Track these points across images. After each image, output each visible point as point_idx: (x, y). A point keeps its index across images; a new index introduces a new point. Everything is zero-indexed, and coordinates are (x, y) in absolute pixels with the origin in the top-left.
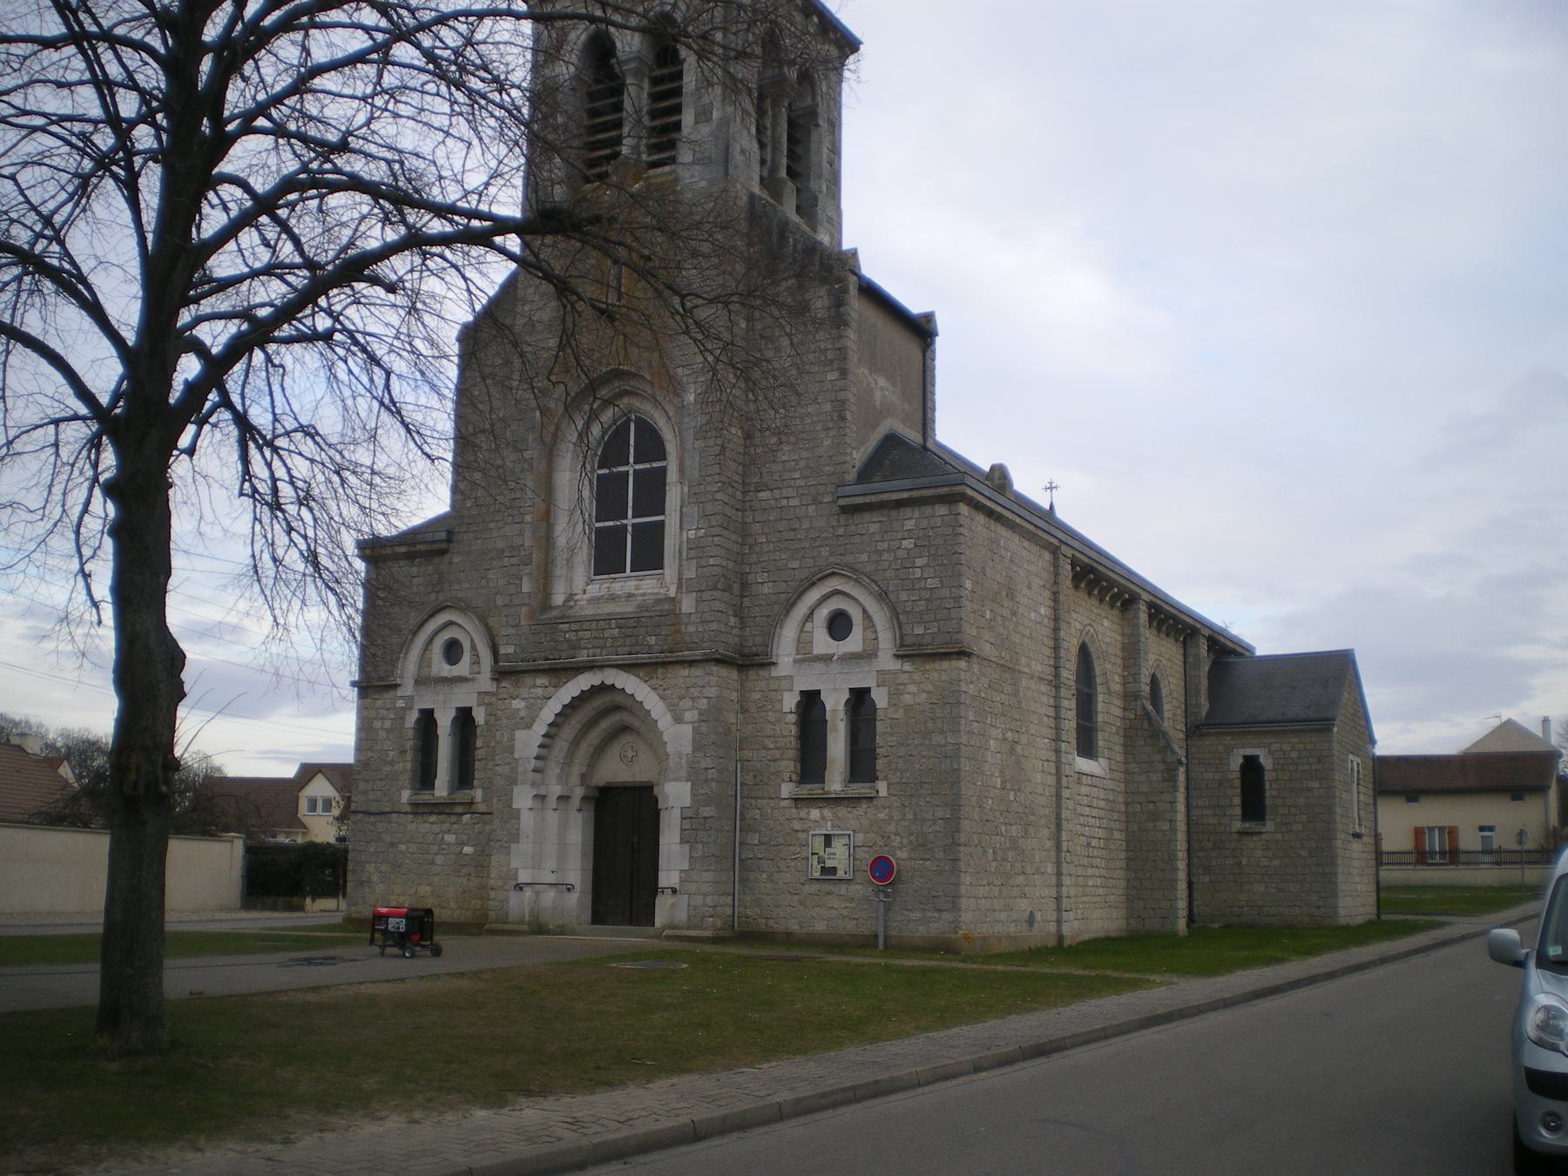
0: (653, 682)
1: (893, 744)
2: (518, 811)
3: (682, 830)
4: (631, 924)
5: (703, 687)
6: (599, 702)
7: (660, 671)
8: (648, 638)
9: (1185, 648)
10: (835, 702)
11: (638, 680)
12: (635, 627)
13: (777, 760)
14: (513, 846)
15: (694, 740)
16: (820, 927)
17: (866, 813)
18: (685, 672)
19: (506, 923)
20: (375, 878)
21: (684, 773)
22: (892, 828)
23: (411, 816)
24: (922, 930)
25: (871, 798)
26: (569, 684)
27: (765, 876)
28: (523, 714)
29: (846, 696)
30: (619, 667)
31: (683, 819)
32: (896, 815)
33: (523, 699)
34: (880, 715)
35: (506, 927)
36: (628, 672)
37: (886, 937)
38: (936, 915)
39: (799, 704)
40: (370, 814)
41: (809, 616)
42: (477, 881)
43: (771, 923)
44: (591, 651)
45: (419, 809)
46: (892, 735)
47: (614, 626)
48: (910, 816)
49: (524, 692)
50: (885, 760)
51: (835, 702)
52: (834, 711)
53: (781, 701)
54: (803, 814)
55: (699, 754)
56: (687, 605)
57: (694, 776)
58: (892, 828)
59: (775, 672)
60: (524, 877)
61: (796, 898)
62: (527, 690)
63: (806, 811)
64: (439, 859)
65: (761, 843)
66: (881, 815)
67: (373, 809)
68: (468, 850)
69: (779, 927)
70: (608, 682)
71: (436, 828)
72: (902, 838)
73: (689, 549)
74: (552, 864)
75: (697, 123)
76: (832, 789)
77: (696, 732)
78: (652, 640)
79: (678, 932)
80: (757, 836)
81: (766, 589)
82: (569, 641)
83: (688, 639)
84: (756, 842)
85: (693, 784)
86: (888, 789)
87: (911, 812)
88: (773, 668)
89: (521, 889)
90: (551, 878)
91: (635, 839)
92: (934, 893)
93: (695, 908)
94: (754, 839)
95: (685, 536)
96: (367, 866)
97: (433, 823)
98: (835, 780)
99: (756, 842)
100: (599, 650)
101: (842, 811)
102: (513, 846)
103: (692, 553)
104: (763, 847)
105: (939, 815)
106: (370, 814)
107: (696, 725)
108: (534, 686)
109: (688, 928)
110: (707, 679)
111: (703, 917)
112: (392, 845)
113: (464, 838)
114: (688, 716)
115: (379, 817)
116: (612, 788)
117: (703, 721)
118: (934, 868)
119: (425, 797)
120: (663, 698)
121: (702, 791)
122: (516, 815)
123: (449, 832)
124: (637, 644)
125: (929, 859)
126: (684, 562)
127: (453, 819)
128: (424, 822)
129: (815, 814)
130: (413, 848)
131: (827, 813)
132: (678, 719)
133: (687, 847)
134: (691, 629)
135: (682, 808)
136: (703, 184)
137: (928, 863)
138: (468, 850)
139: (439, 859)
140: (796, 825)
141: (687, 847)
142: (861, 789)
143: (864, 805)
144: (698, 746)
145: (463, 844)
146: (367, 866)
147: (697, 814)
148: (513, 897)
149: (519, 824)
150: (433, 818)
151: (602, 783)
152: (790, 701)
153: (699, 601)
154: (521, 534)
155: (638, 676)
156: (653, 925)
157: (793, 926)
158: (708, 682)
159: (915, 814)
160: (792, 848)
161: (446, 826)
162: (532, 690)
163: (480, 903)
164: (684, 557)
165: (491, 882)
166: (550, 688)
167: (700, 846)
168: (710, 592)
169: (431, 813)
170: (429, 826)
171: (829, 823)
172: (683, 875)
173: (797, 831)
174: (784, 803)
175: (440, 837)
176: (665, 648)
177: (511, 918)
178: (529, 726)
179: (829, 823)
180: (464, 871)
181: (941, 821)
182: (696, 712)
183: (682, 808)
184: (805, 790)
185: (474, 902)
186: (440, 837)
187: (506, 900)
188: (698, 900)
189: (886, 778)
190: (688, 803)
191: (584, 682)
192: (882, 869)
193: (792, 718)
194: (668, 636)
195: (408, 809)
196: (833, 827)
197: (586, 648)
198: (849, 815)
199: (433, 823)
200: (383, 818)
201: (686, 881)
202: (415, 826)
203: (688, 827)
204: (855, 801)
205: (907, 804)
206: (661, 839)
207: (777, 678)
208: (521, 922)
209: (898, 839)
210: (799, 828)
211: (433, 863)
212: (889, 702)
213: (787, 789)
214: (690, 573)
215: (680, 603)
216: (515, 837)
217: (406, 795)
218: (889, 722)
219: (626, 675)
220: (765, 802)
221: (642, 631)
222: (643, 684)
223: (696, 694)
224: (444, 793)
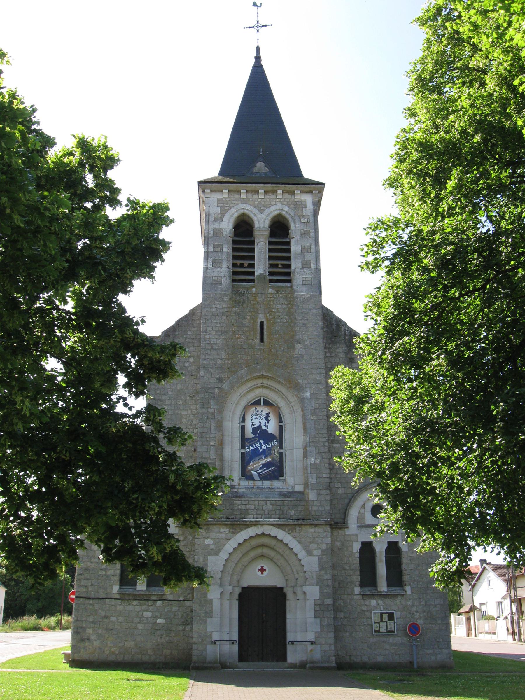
0: (294, 534)
1: (412, 568)
2: (211, 600)
3: (315, 611)
4: (263, 661)
5: (324, 538)
6: (260, 541)
7: (298, 528)
8: (290, 511)
9: (344, 519)
10: (380, 548)
11: (285, 533)
12: (281, 505)
13: (350, 576)
14: (209, 620)
15: (319, 564)
16: (380, 659)
17: (401, 602)
18: (312, 530)
19: (205, 663)
20: (93, 637)
21: (314, 581)
22: (414, 609)
23: (119, 602)
24: (433, 658)
25: (403, 595)
26: (241, 532)
27: (348, 634)
28: (212, 547)
29: (386, 545)
30: (273, 525)
31: (315, 605)
32: (416, 602)
33: (212, 539)
34: (404, 555)
35: (205, 665)
36: (278, 528)
37: (418, 663)
38: (440, 650)
39: (361, 549)
40: (90, 598)
41: (363, 506)
42: (167, 638)
43: (353, 658)
44: (255, 516)
45: (123, 598)
46: (411, 564)
47: (268, 504)
48: (423, 603)
49: (213, 535)
50: (408, 576)
51: (380, 548)
52: (381, 552)
53: (352, 546)
54: (367, 603)
55: (323, 572)
56: (312, 496)
57: (320, 582)
58: (414, 609)
59: (347, 532)
60: (215, 637)
61: (366, 644)
62: (214, 534)
63: (369, 601)
64: (140, 626)
65: (345, 617)
66: (409, 603)
67: (93, 596)
68: (159, 621)
69: (358, 660)
70: (266, 532)
71: (138, 608)
72: (420, 614)
73: (311, 468)
74: (227, 629)
75: (303, 268)
76: (382, 590)
77: (320, 560)
78: (292, 513)
79: (315, 665)
80: (343, 613)
81: (340, 491)
82: (240, 510)
83: (313, 513)
84: (342, 617)
85: (320, 587)
86: (411, 590)
87: (424, 601)
88: (346, 529)
89: (215, 643)
90: (226, 637)
91: (264, 615)
92: (438, 640)
93: (325, 651)
94: (342, 615)
95: (308, 461)
96: (87, 629)
97: (136, 605)
98: (383, 586)
99: (342, 617)
100: (260, 516)
101: (388, 601)
102: (209, 620)
103: (313, 470)
104: (346, 619)
105: (438, 601)
106: (90, 598)
107: (320, 557)
108: (220, 532)
109: (322, 663)
110: (325, 534)
111: (329, 657)
112: (106, 617)
113: (158, 614)
114: (315, 552)
115: (97, 601)
116: (252, 588)
117: (324, 555)
118: (437, 628)
119: (128, 590)
120: (299, 542)
121: (326, 591)
122: (211, 602)
123: (147, 610)
124: (283, 514)
125: (434, 624)
126: (309, 475)
127: (150, 603)
128: (129, 604)
129: (374, 602)
130: (121, 619)
131: (380, 602)
132: (310, 553)
133: (318, 620)
134: (315, 508)
135: (314, 599)
136: (309, 296)
137: (433, 626)
138: (159, 621)
139: (140, 626)
140: (364, 608)
141: (318, 620)
142: (396, 590)
143: (399, 598)
144: (322, 568)
145: (157, 617)
146: (87, 629)
147: (323, 603)
148: (210, 648)
149: (212, 607)
150: (135, 603)
151: (245, 585)
152: (357, 547)
153: (319, 495)
154: (208, 451)
155: (285, 531)
156: (285, 659)
157: (365, 659)
158: (326, 536)
159: (426, 602)
160: (362, 620)
161: (144, 608)
162: (218, 534)
163: (169, 651)
164: (309, 472)
165: (194, 640)
166: (229, 534)
167: (326, 619)
168: (324, 491)
169: (135, 599)
170: (134, 606)
171: (381, 607)
172: (317, 634)
173: (364, 611)
174: (358, 597)
175: (140, 613)
176: (300, 517)
177: (208, 659)
178: (216, 553)
179: (381, 607)
180: (158, 633)
181: (439, 606)
182: (320, 551)
183: (314, 599)
184: (367, 591)
185: (165, 651)
186: (140, 613)
187: (205, 649)
188: (326, 648)
189: (410, 585)
190: (318, 596)
191: (251, 531)
192: (414, 628)
193: (357, 555)
194: (301, 511)
195: (118, 597)
196: (384, 609)
197: (252, 514)
198: (392, 603)
199: (136, 605)
200: (100, 601)
201: (318, 638)
202: (120, 607)
203: (318, 609)
204: (395, 596)
205: (421, 597)
206: (289, 617)
207: (349, 535)
208: (215, 662)
209: (418, 614)
210: (366, 609)
211: (136, 628)
212: (409, 549)
213: (357, 590)
214: (313, 480)
215: (308, 495)
216: (209, 614)
217: (116, 589)
218: (409, 558)
219: (277, 529)
220: (346, 596)
221: (286, 508)
222: (287, 535)
223: (319, 541)
224: (144, 588)
